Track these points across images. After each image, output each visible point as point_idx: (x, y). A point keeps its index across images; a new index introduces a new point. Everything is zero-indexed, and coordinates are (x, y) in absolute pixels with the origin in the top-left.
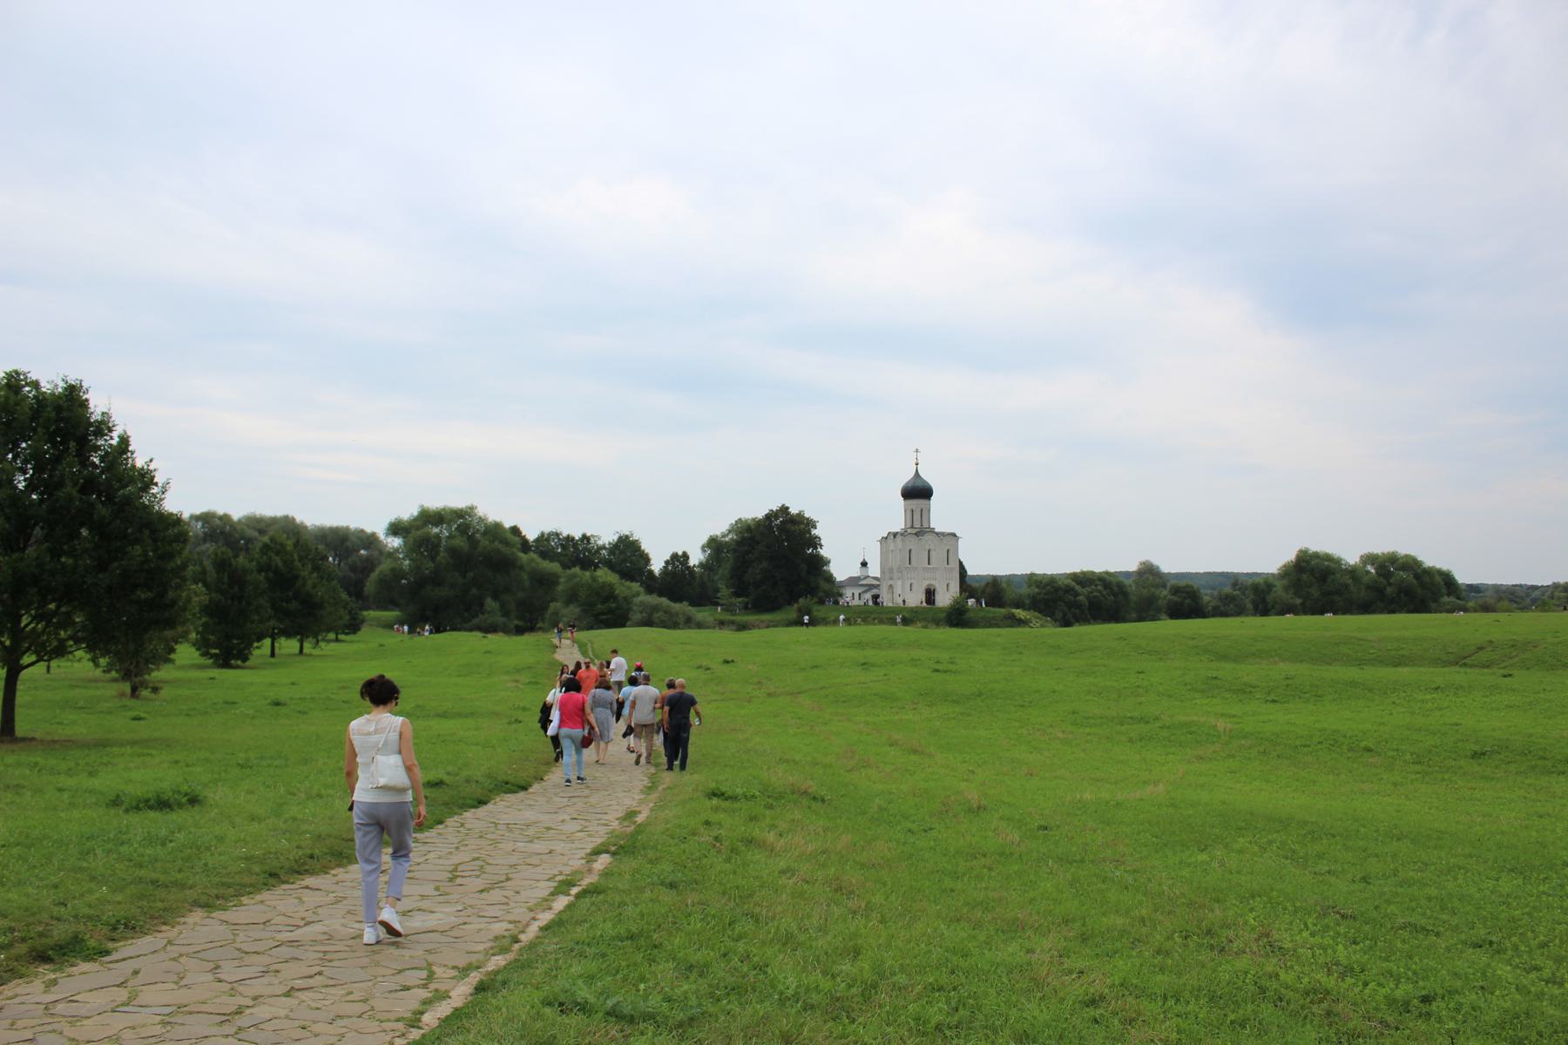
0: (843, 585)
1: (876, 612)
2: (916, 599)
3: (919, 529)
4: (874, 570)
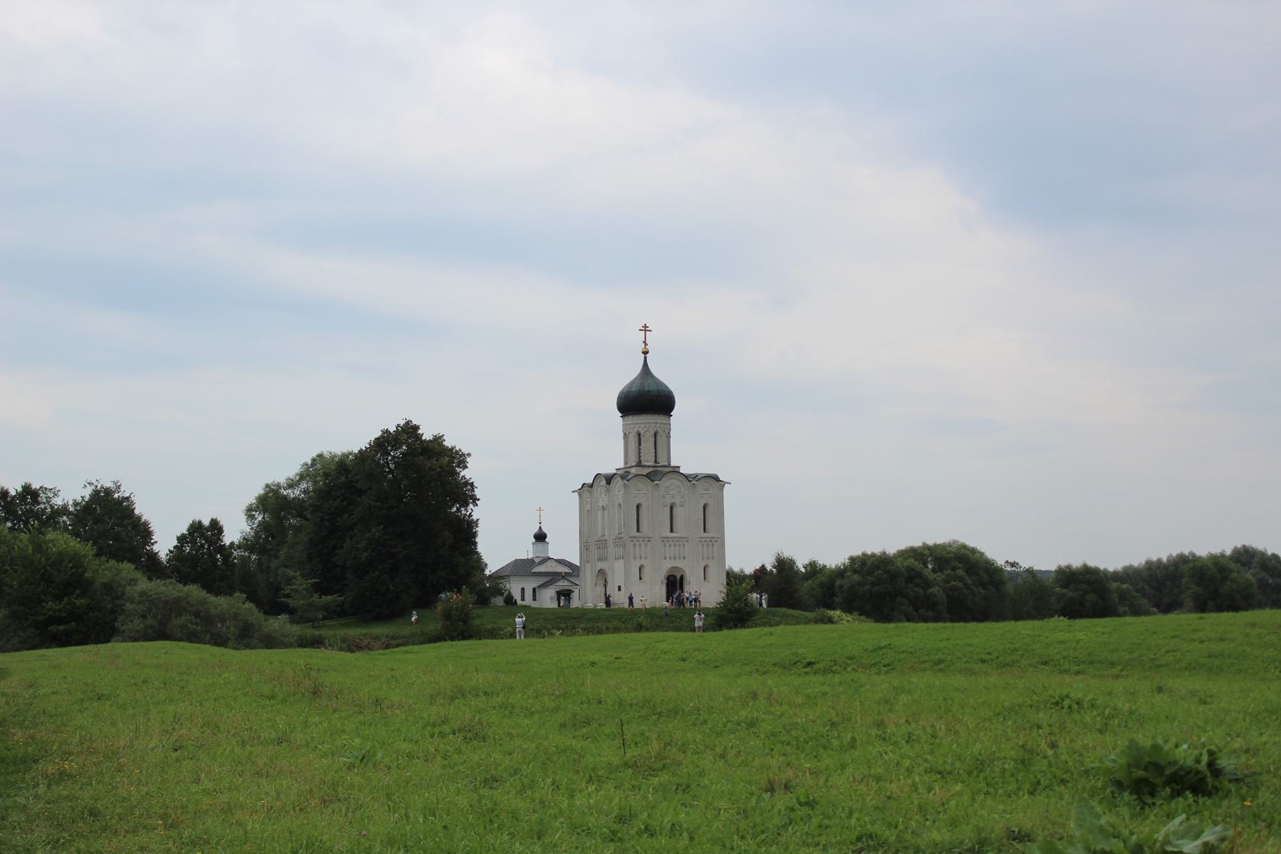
0: (498, 576)
1: (568, 621)
2: (652, 595)
3: (650, 468)
4: (565, 547)
